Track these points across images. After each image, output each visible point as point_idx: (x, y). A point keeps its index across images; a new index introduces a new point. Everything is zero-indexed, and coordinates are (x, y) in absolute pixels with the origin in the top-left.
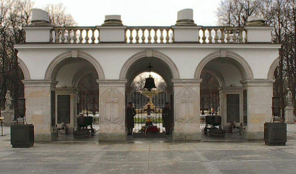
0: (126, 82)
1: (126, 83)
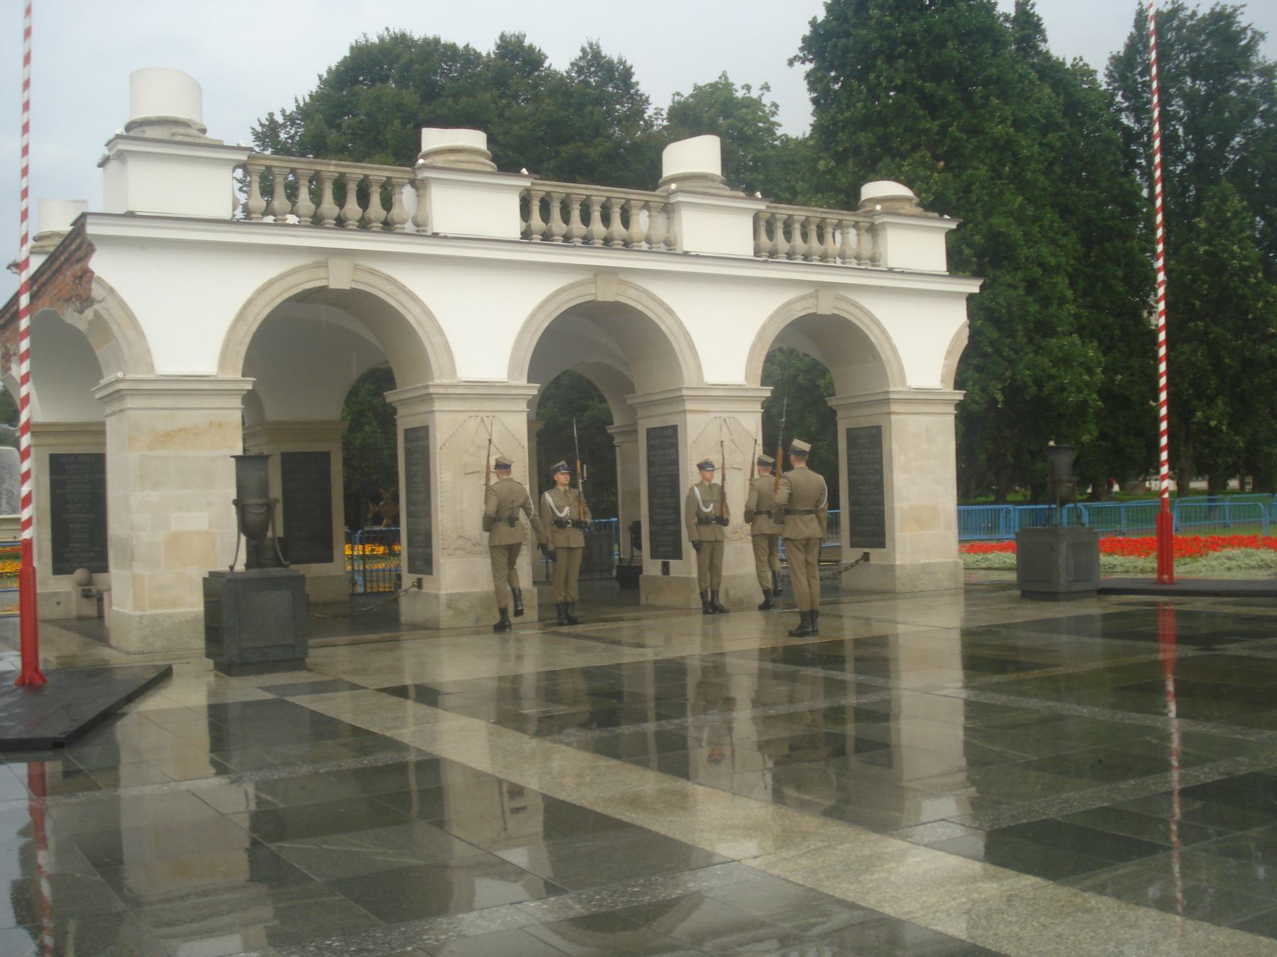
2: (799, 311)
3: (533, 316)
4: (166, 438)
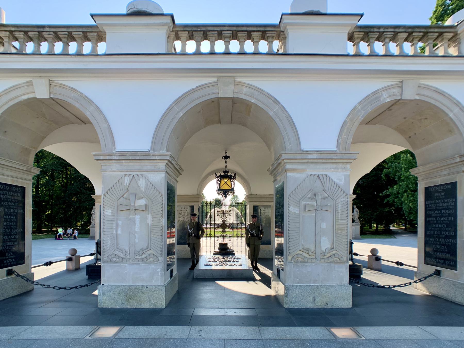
1: (169, 160)
3: (170, 109)
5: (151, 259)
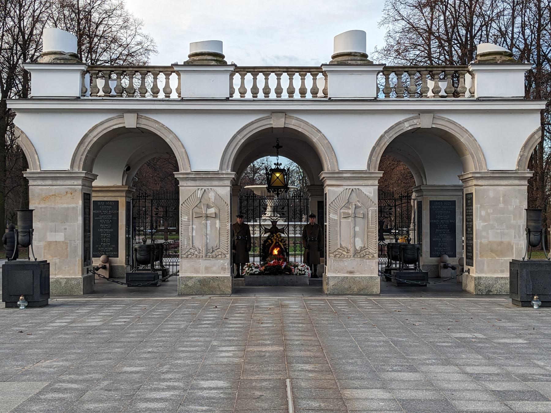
0: (233, 177)
1: (233, 178)
2: (407, 127)
4: (45, 199)
5: (220, 256)
